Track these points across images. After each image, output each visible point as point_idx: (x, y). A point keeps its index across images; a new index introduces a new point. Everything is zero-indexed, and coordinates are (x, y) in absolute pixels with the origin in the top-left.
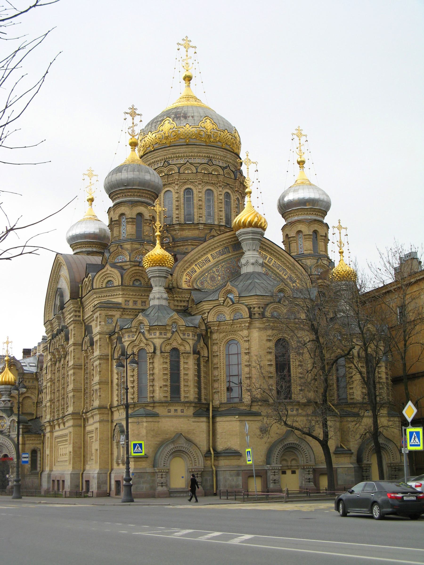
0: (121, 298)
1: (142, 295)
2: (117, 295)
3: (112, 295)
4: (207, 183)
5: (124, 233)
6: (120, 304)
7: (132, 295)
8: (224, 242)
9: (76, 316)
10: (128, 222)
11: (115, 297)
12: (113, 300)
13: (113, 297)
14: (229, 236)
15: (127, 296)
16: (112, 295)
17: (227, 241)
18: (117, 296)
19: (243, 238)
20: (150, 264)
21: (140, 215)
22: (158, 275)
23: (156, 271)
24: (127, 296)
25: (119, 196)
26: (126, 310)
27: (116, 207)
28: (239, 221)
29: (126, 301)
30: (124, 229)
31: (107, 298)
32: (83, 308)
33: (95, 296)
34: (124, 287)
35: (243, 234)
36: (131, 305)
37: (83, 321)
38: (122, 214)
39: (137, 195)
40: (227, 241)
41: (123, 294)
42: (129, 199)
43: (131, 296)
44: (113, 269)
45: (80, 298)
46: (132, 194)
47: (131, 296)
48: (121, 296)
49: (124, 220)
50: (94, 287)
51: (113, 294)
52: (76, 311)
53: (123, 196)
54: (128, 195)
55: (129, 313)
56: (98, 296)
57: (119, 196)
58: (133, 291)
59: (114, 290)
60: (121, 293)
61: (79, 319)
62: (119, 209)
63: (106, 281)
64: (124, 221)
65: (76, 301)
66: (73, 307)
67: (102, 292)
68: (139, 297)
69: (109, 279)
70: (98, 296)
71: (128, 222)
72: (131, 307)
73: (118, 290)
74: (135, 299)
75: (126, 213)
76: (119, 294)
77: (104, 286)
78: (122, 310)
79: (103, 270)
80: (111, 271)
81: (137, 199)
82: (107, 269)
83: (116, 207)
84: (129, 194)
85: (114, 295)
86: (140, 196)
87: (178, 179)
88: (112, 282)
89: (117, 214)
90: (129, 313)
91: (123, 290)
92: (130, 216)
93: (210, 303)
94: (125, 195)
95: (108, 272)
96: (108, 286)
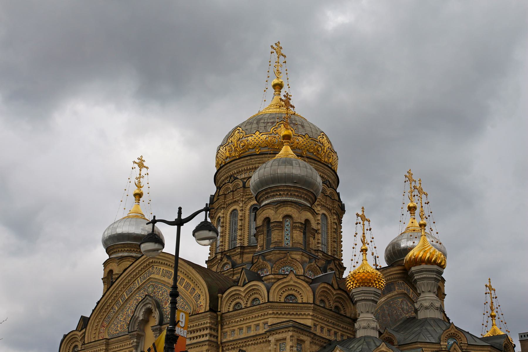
0: (310, 320)
1: (328, 322)
2: (305, 314)
3: (297, 314)
4: (323, 206)
5: (287, 239)
6: (310, 327)
7: (320, 319)
8: (393, 276)
9: (211, 335)
10: (294, 228)
11: (301, 317)
12: (298, 321)
13: (297, 317)
14: (397, 270)
15: (315, 319)
16: (297, 314)
17: (395, 276)
18: (305, 317)
19: (424, 276)
20: (356, 284)
21: (307, 221)
22: (363, 298)
23: (361, 293)
24: (315, 319)
25: (282, 193)
26: (317, 338)
27: (279, 206)
28: (411, 258)
29: (315, 325)
30: (288, 234)
31: (289, 316)
32: (222, 326)
33: (270, 312)
34: (316, 307)
35: (426, 271)
36: (318, 332)
37: (221, 343)
38: (288, 216)
39: (304, 197)
40: (395, 276)
41: (312, 316)
42: (295, 199)
43: (318, 320)
44: (299, 281)
45: (220, 312)
46: (300, 195)
47: (318, 320)
48: (310, 317)
49: (287, 223)
50: (271, 300)
51: (299, 313)
52: (211, 328)
53: (287, 194)
54: (295, 195)
55: (317, 342)
56: (275, 312)
57: (282, 193)
58: (322, 314)
59: (302, 308)
60: (311, 314)
61: (215, 340)
62: (283, 209)
63: (286, 294)
64: (288, 225)
65: (215, 315)
66: (210, 323)
67: (282, 308)
68: (326, 323)
69: (293, 292)
70: (275, 312)
71: (294, 228)
72: (318, 334)
73: (308, 309)
74: (322, 325)
75: (293, 215)
76: (309, 314)
77: (282, 300)
78: (312, 336)
79: (285, 280)
80: (295, 282)
81: (304, 202)
82: (291, 279)
83: (279, 206)
84: (297, 194)
85: (301, 314)
86: (306, 200)
87: (243, 195)
88: (293, 298)
89: (280, 214)
90: (317, 342)
91: (314, 310)
92: (299, 221)
93: (428, 346)
94: (291, 194)
95: (291, 283)
96: (287, 301)
